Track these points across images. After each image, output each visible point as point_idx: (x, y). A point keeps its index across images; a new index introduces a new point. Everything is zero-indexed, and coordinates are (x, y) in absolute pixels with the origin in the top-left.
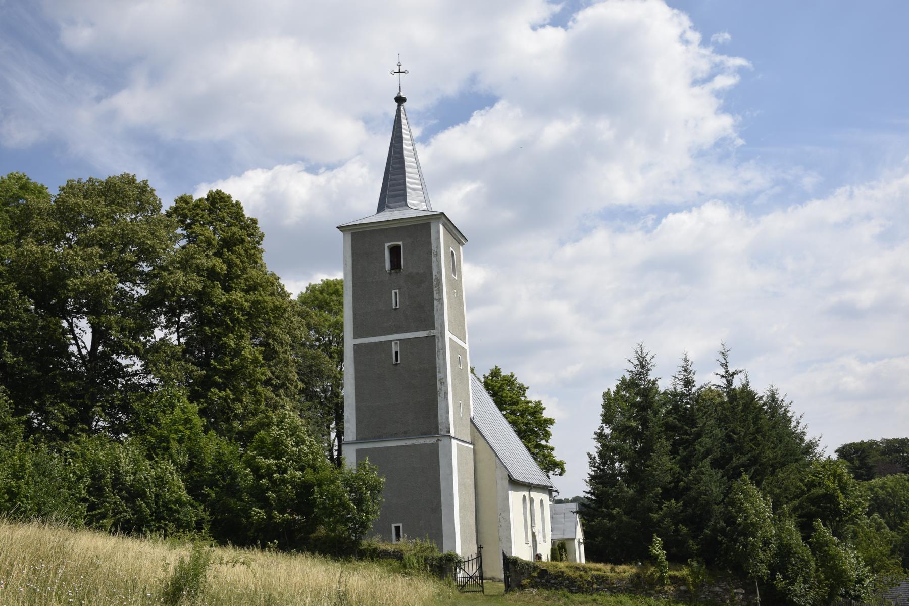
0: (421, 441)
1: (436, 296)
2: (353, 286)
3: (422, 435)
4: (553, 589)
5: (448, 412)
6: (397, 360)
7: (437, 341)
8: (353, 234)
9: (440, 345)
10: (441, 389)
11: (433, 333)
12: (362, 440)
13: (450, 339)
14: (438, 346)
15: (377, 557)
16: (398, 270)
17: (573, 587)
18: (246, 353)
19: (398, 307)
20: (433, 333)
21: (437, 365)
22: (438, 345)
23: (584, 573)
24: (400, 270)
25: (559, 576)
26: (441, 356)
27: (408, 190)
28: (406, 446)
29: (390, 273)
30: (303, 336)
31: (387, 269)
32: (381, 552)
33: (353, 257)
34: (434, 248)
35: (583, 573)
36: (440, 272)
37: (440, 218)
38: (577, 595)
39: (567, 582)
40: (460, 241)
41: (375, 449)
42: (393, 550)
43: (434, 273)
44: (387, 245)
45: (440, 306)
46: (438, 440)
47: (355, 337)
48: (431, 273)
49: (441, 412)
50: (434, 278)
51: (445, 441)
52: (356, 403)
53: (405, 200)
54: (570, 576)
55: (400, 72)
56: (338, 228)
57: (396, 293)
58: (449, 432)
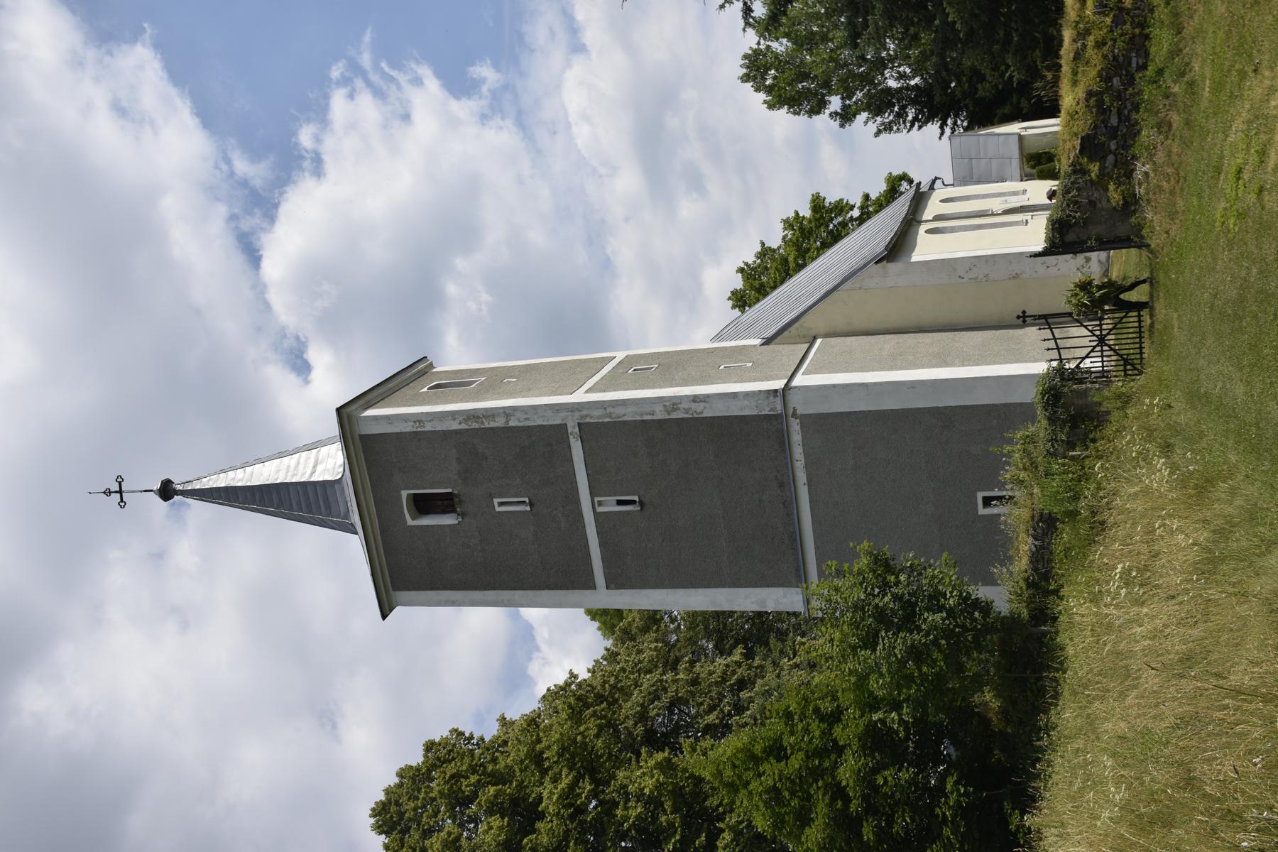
0: (798, 452)
1: (500, 422)
2: (493, 588)
3: (784, 450)
4: (1134, 116)
5: (734, 395)
6: (632, 502)
7: (588, 420)
8: (397, 588)
9: (596, 413)
10: (687, 411)
11: (573, 429)
12: (800, 576)
13: (587, 392)
14: (599, 417)
15: (1047, 580)
16: (456, 500)
17: (1130, 64)
18: (649, 784)
19: (527, 500)
20: (573, 429)
21: (639, 418)
22: (596, 416)
23: (1091, 38)
24: (458, 496)
25: (1100, 103)
26: (619, 411)
27: (314, 479)
28: (810, 483)
29: (463, 515)
30: (653, 646)
31: (457, 522)
32: (1035, 570)
33: (438, 589)
34: (408, 428)
35: (1091, 40)
36: (453, 414)
37: (349, 417)
38: (1153, 50)
39: (1116, 81)
40: (419, 371)
41: (817, 548)
42: (1030, 540)
43: (455, 426)
44: (410, 522)
45: (518, 414)
46: (794, 415)
47: (594, 587)
48: (456, 432)
49: (735, 410)
50: (464, 426)
51: (795, 401)
52: (723, 586)
53: (332, 483)
54: (1099, 75)
55: (120, 492)
56: (384, 617)
57: (501, 504)
58: (776, 391)
